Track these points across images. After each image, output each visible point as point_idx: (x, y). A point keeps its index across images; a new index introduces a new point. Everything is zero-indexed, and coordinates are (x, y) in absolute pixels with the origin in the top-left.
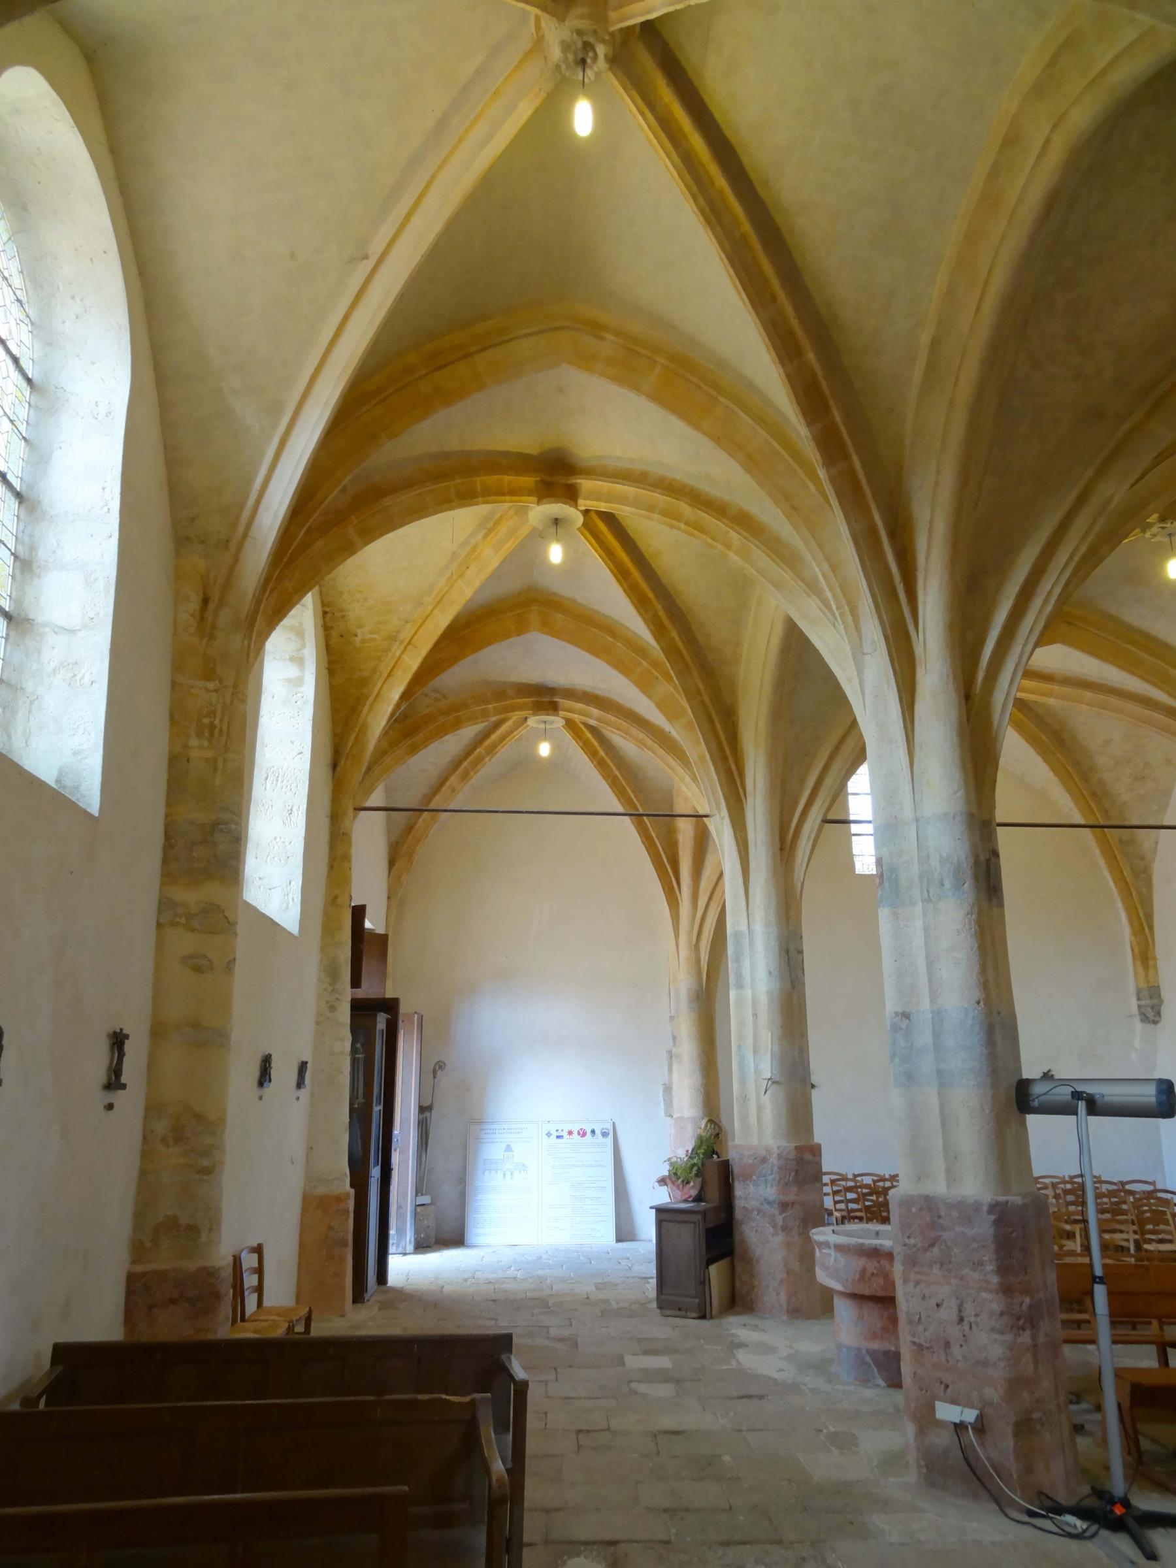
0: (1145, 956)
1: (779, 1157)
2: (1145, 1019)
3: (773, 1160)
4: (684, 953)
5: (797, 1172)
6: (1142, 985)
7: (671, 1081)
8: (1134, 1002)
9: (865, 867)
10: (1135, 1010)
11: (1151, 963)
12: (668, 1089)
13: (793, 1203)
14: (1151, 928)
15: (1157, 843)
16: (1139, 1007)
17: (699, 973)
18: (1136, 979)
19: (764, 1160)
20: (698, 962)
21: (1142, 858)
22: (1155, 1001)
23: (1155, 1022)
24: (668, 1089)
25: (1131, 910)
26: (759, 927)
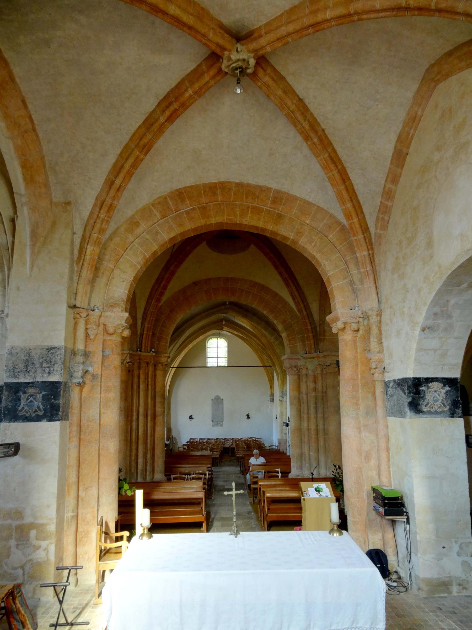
2: (271, 401)
14: (273, 380)
25: (268, 376)
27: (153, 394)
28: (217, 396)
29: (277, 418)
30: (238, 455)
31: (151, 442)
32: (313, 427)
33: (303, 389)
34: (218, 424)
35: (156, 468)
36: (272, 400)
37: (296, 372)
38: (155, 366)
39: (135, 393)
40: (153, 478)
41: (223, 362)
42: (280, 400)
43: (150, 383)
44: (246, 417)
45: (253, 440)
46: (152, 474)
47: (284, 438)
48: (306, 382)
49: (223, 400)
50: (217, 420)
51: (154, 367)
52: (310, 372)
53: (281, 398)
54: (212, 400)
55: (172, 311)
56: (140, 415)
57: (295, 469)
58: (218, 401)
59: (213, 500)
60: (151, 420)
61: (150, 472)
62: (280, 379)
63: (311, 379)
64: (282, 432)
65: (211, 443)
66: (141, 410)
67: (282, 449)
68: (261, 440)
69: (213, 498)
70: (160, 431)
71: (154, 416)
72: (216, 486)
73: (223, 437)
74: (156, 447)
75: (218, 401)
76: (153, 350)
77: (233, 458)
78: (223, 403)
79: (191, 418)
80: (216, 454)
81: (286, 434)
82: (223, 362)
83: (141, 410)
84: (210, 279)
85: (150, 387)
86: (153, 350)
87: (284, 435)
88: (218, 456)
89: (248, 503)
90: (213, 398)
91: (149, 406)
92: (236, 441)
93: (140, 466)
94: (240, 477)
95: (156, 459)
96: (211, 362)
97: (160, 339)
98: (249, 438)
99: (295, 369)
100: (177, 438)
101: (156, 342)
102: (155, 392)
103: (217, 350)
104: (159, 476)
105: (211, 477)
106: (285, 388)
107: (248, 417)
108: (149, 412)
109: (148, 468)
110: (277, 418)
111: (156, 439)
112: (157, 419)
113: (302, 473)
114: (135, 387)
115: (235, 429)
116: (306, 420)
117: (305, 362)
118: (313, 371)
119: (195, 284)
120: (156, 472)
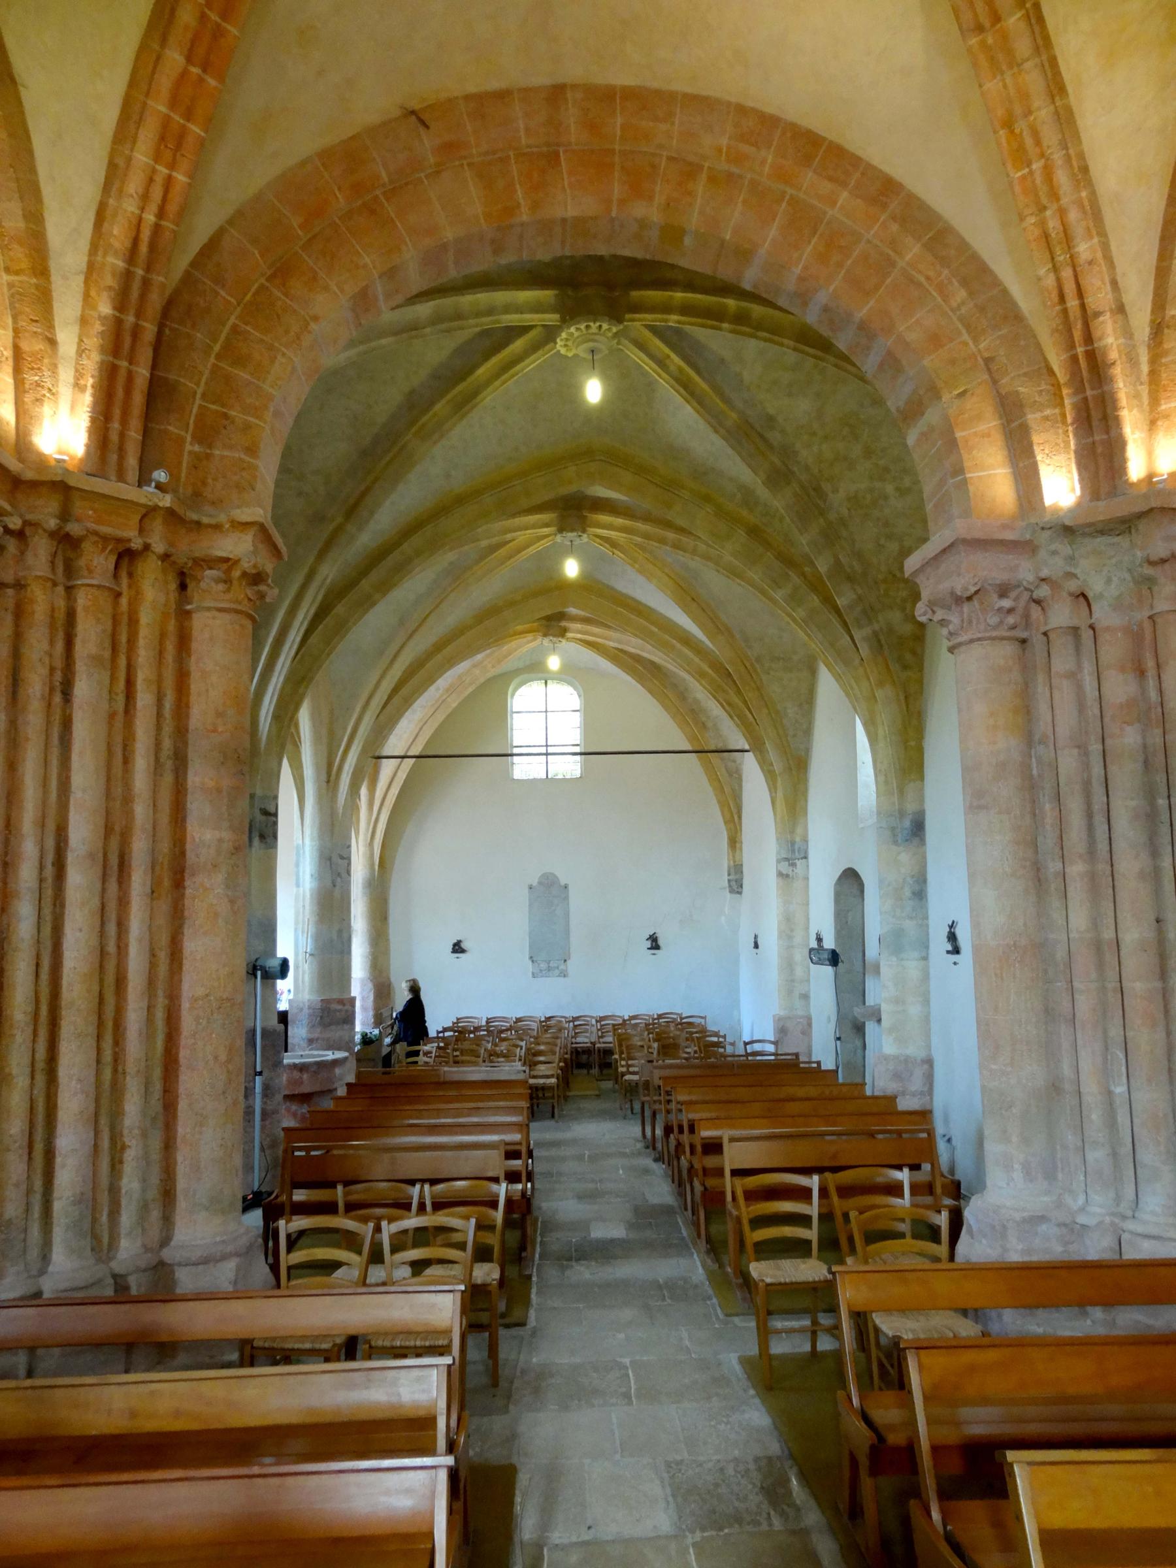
0: (734, 842)
1: (309, 1008)
3: (306, 1011)
8: (726, 878)
11: (738, 845)
14: (740, 817)
17: (372, 865)
19: (301, 1010)
25: (723, 804)
26: (307, 841)
27: (167, 744)
28: (546, 876)
29: (756, 946)
30: (627, 1077)
31: (150, 1020)
32: (1134, 933)
33: (1061, 714)
34: (549, 969)
35: (181, 1184)
36: (736, 886)
37: (1011, 620)
38: (183, 587)
39: (34, 720)
40: (165, 1241)
42: (780, 874)
43: (142, 676)
45: (674, 1021)
46: (155, 1214)
47: (800, 1013)
48: (1073, 675)
49: (566, 887)
50: (549, 955)
51: (173, 586)
52: (1103, 614)
54: (530, 888)
55: (282, 272)
56: (71, 858)
57: (1018, 1175)
58: (549, 893)
59: (534, 1332)
60: (153, 894)
61: (144, 1208)
62: (780, 794)
63: (1113, 650)
64: (790, 992)
65: (526, 1031)
66: (82, 833)
67: (789, 1048)
68: (703, 1021)
69: (532, 1320)
70: (207, 957)
71: (175, 874)
72: (550, 1226)
73: (571, 1013)
74: (183, 1054)
75: (549, 893)
76: (161, 476)
77: (608, 1085)
78: (567, 898)
79: (458, 948)
80: (547, 1074)
81: (805, 997)
83: (82, 833)
84: (502, 96)
85: (144, 699)
86: (161, 476)
88: (553, 1080)
89: (731, 1361)
90: (535, 883)
91: (141, 811)
92: (621, 1028)
93: (68, 1176)
94: (646, 1171)
95: (183, 1128)
97: (207, 433)
98: (660, 1016)
99: (1006, 603)
101: (191, 447)
102: (181, 732)
104: (210, 1229)
105: (524, 1193)
106: (799, 830)
107: (654, 943)
108: (139, 847)
109: (130, 1183)
110: (756, 946)
111: (185, 1005)
112: (191, 886)
113: (1059, 1204)
114: (35, 684)
115: (613, 989)
116: (1077, 892)
117: (1071, 559)
118: (1118, 605)
119: (417, 117)
120: (182, 1204)
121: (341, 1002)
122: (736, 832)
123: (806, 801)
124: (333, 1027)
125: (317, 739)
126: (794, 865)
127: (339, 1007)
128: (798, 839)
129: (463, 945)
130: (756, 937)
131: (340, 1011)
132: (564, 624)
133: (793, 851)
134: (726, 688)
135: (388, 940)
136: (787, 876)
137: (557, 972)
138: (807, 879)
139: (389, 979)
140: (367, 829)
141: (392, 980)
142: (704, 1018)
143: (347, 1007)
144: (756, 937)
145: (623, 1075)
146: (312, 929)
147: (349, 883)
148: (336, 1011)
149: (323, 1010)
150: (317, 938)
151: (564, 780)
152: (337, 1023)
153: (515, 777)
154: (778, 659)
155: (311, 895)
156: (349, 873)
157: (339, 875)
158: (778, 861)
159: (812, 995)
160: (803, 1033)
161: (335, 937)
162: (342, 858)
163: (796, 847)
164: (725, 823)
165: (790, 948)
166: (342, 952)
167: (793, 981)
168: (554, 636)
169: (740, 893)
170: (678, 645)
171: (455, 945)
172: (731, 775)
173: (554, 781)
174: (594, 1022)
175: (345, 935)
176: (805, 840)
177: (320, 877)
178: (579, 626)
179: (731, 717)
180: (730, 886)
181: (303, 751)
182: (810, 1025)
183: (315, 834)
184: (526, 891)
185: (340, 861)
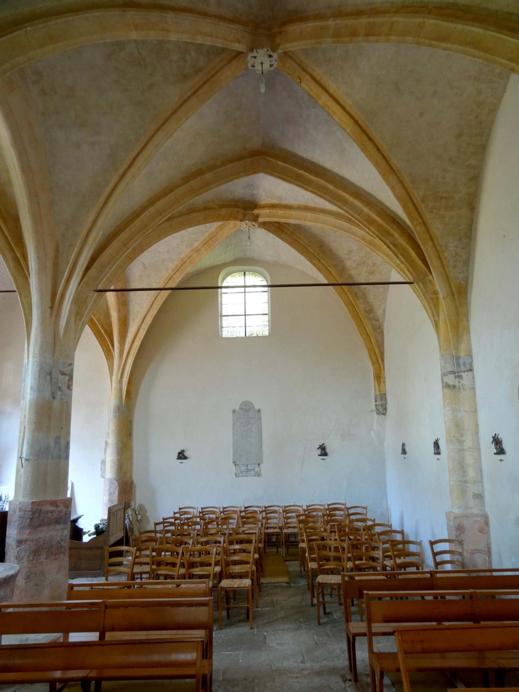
0: (379, 377)
1: (20, 510)
2: (379, 413)
3: (18, 513)
4: (114, 385)
5: (31, 519)
6: (378, 393)
7: (105, 458)
8: (374, 403)
9: (229, 333)
10: (374, 408)
11: (382, 380)
12: (103, 463)
13: (26, 540)
14: (383, 360)
15: (385, 311)
16: (376, 405)
18: (375, 391)
20: (121, 390)
21: (378, 320)
22: (383, 402)
23: (385, 414)
24: (103, 463)
25: (371, 350)
26: (31, 359)
29: (404, 452)
34: (248, 471)
41: (260, 326)
42: (446, 386)
44: (319, 452)
47: (475, 511)
49: (259, 411)
50: (247, 461)
53: (451, 380)
54: (234, 411)
64: (463, 492)
75: (247, 416)
78: (260, 419)
79: (182, 456)
81: (479, 496)
82: (260, 326)
87: (472, 502)
90: (237, 408)
96: (231, 328)
100: (147, 508)
103: (244, 306)
106: (463, 347)
107: (323, 451)
110: (404, 452)
115: (294, 485)
121: (54, 503)
122: (380, 370)
123: (468, 321)
124: (43, 528)
125: (41, 269)
126: (460, 377)
127: (52, 508)
128: (462, 354)
129: (186, 454)
130: (404, 445)
131: (52, 512)
132: (256, 212)
133: (459, 365)
134: (392, 231)
135: (131, 451)
136: (454, 387)
137: (253, 473)
138: (473, 389)
139: (131, 478)
140: (119, 370)
141: (135, 480)
142: (365, 508)
143: (61, 508)
144: (404, 445)
145: (315, 573)
146: (28, 436)
147: (70, 396)
148: (48, 512)
149: (33, 512)
150: (32, 445)
151: (258, 337)
152: (49, 524)
153: (224, 336)
154: (442, 198)
155: (30, 406)
156: (69, 387)
157: (59, 388)
158: (444, 375)
159: (487, 495)
160: (481, 531)
161: (52, 445)
162: (63, 374)
163: (461, 362)
164: (373, 364)
165: (461, 450)
166: (59, 457)
167: (465, 482)
168: (249, 220)
169: (385, 414)
170: (351, 199)
171: (179, 453)
172: (375, 330)
173: (251, 338)
174: (281, 510)
175: (63, 443)
176: (470, 355)
177: (39, 389)
178: (267, 211)
179: (397, 256)
180: (377, 409)
181: (31, 282)
182: (487, 523)
183: (37, 352)
184: (231, 413)
185: (61, 377)
